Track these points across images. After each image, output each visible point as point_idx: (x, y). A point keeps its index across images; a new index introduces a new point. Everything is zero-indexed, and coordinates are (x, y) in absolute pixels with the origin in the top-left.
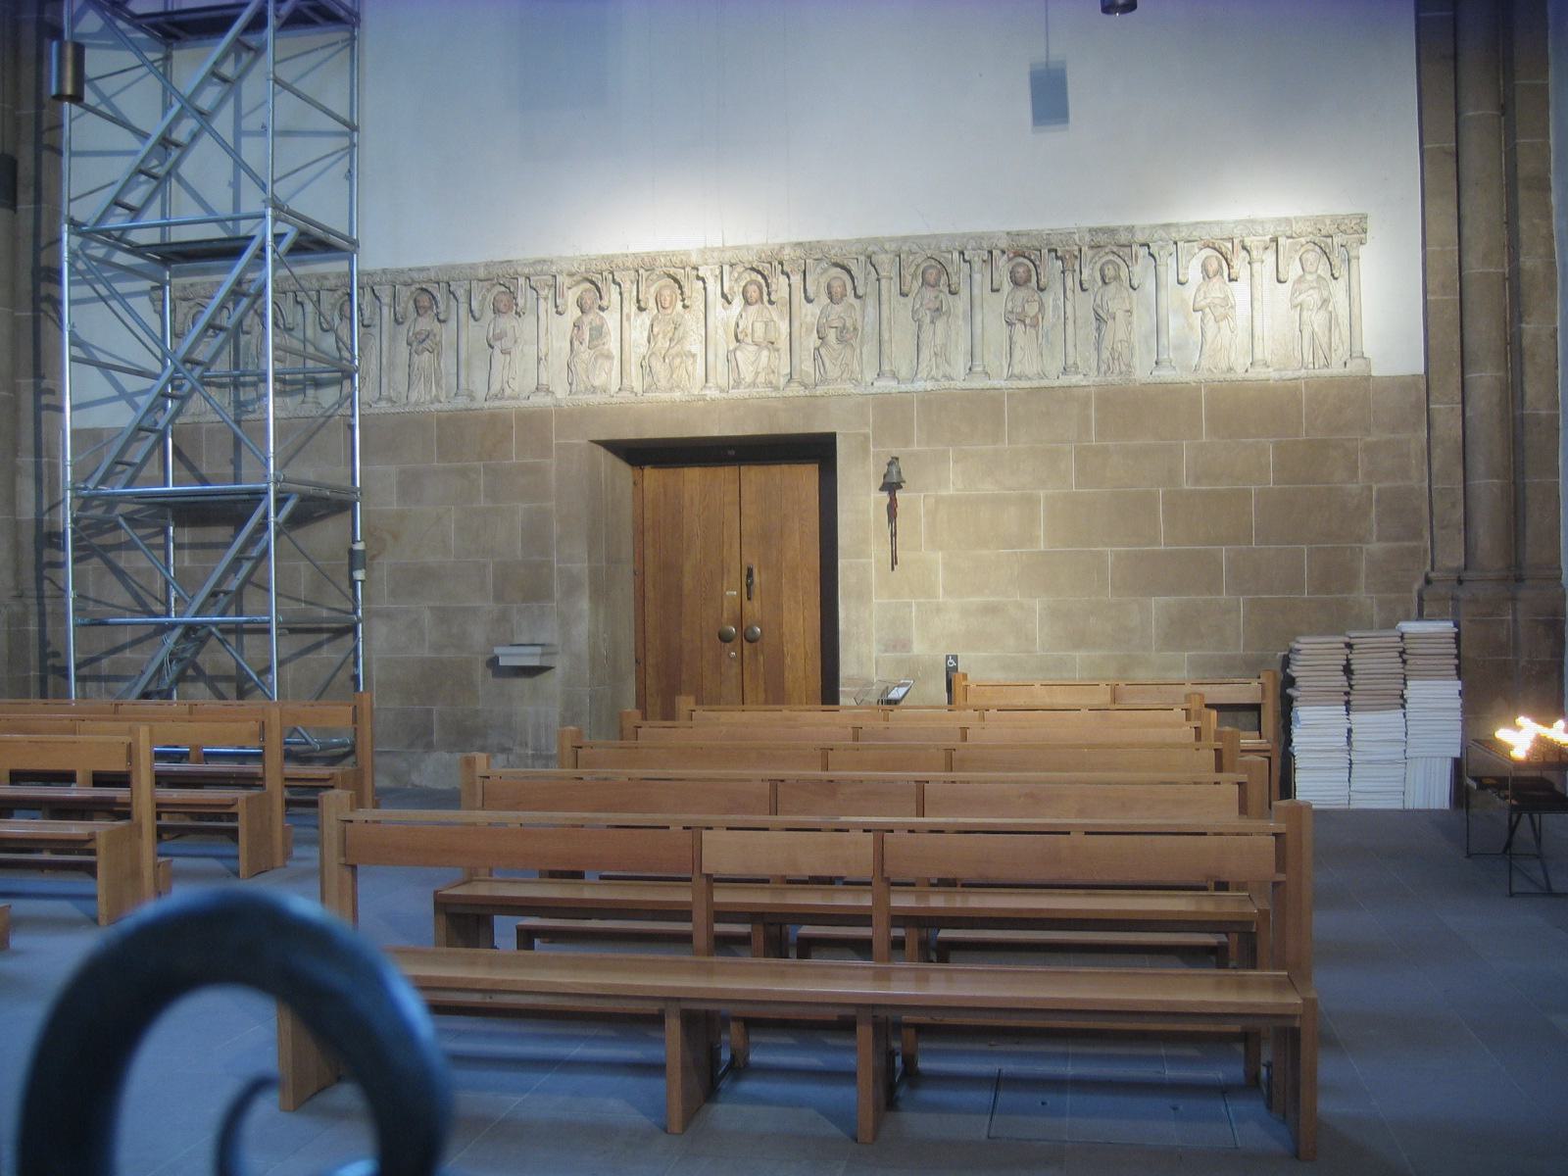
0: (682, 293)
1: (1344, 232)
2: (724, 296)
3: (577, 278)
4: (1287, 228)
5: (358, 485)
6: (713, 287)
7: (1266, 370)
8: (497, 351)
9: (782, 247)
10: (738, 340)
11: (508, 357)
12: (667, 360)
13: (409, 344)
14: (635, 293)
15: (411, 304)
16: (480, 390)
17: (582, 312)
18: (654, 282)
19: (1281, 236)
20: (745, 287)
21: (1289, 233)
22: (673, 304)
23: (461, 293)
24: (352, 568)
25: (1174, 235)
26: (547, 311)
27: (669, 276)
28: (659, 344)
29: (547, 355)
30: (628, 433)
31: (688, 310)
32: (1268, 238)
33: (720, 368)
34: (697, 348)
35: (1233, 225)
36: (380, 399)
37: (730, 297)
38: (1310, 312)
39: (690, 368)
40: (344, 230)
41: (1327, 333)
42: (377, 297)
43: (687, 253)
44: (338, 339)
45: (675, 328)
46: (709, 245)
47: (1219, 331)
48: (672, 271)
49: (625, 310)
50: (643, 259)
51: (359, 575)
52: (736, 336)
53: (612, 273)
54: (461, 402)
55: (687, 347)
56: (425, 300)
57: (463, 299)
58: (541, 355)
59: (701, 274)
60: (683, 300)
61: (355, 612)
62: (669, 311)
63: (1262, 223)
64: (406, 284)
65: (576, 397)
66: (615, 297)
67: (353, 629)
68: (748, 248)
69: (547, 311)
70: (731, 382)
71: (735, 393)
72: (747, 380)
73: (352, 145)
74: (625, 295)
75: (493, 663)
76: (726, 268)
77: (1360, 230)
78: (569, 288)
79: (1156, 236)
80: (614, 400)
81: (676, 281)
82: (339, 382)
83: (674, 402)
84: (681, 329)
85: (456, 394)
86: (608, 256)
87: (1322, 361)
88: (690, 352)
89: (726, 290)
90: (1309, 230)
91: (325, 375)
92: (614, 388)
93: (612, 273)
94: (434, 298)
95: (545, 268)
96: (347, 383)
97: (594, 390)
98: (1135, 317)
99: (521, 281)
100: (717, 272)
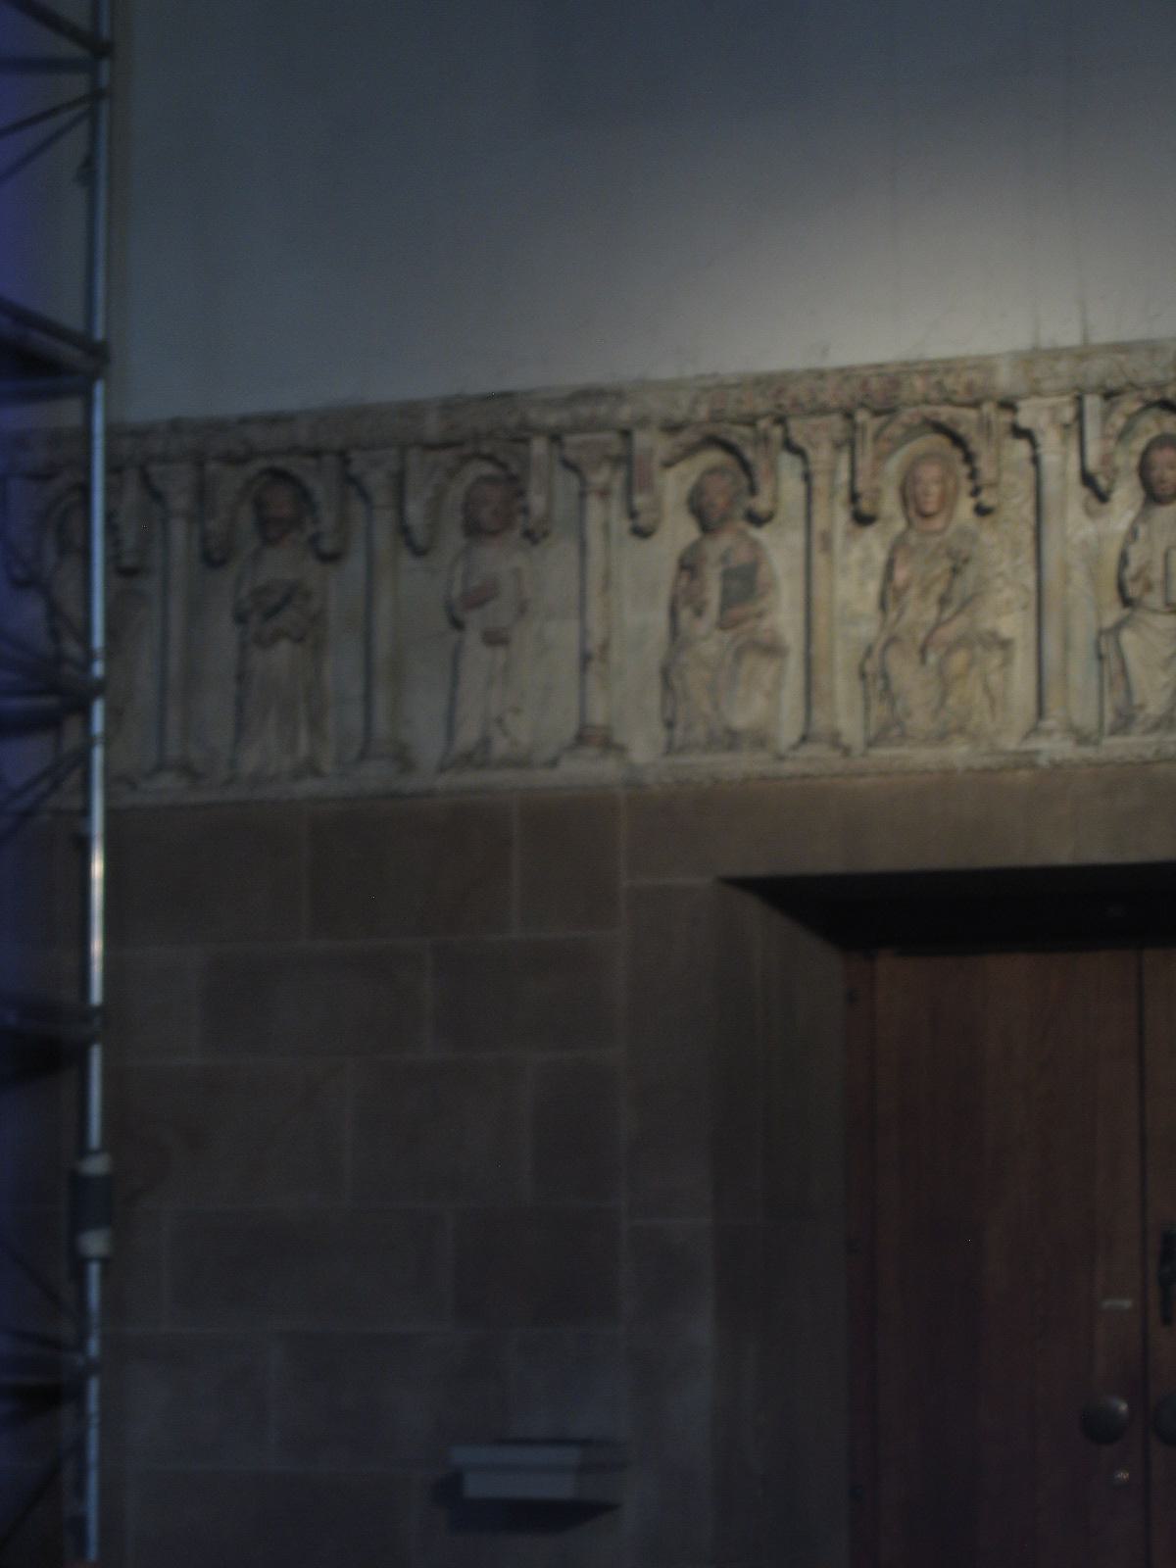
0: (973, 475)
2: (1087, 479)
3: (688, 437)
5: (96, 996)
6: (1058, 457)
8: (472, 638)
10: (1127, 602)
11: (500, 654)
12: (932, 659)
13: (241, 618)
14: (844, 476)
15: (246, 517)
16: (429, 749)
17: (707, 527)
18: (897, 444)
20: (1145, 455)
22: (947, 502)
23: (377, 480)
24: (77, 1227)
26: (606, 528)
27: (939, 428)
28: (910, 614)
29: (605, 647)
30: (824, 857)
31: (987, 521)
33: (1081, 672)
34: (1014, 624)
36: (160, 767)
37: (1102, 482)
39: (995, 679)
40: (70, 316)
42: (157, 496)
43: (984, 365)
44: (54, 611)
45: (955, 571)
46: (1045, 343)
48: (945, 413)
49: (820, 523)
50: (865, 384)
51: (95, 1243)
52: (1121, 588)
53: (781, 421)
54: (374, 776)
55: (987, 623)
56: (281, 502)
57: (382, 498)
58: (594, 643)
59: (1024, 419)
60: (975, 492)
61: (81, 1345)
62: (937, 523)
64: (233, 460)
66: (791, 487)
67: (79, 1395)
68: (1152, 348)
69: (606, 528)
70: (1109, 717)
71: (1117, 747)
73: (96, 95)
74: (820, 482)
75: (448, 1489)
76: (1093, 403)
78: (668, 465)
80: (788, 767)
81: (958, 441)
82: (50, 722)
83: (948, 772)
84: (970, 573)
85: (363, 756)
88: (994, 634)
89: (1093, 463)
91: (17, 704)
92: (788, 732)
93: (781, 421)
94: (304, 495)
95: (603, 410)
96: (72, 726)
97: (732, 740)
100: (1068, 414)
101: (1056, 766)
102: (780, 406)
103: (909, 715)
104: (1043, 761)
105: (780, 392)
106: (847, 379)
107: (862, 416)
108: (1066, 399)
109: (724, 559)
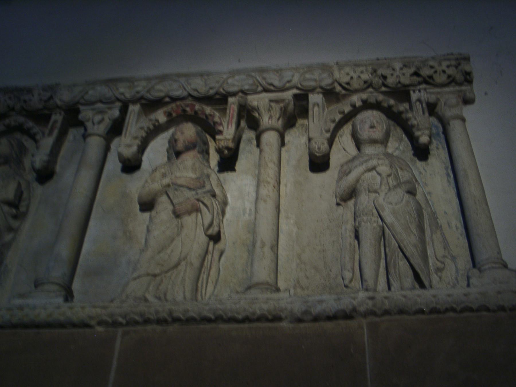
1: (428, 81)
4: (325, 75)
7: (275, 296)
19: (313, 90)
21: (326, 82)
25: (122, 90)
32: (288, 95)
35: (225, 77)
38: (373, 195)
41: (413, 228)
47: (178, 235)
63: (278, 71)
77: (459, 77)
79: (91, 92)
87: (409, 280)
90: (365, 77)
98: (27, 225)
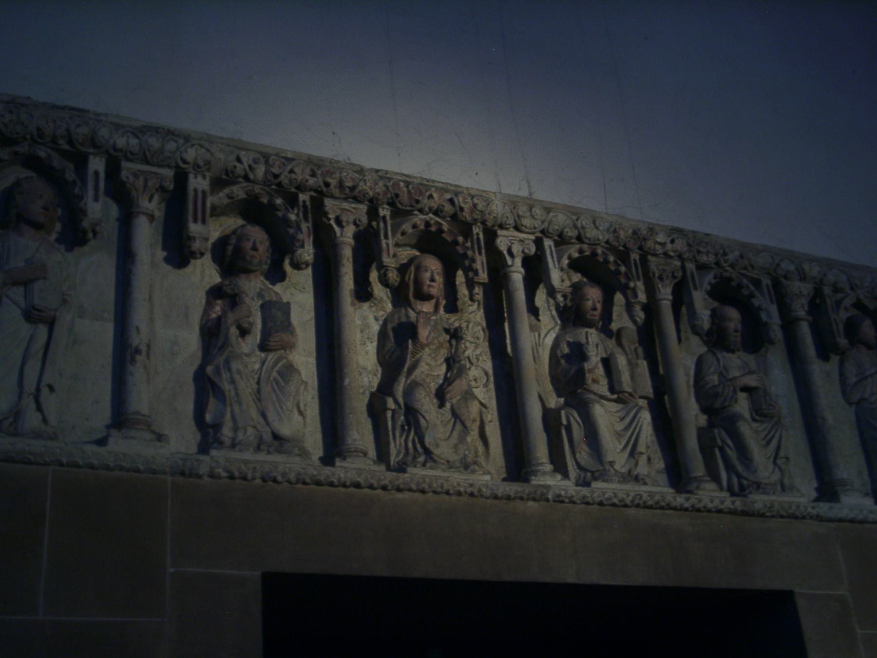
9: (651, 230)
28: (423, 368)
43: (483, 195)
65: (236, 455)
72: (617, 467)
86: (321, 159)
95: (171, 146)
99: (97, 164)
101: (559, 500)
102: (327, 185)
103: (437, 446)
104: (550, 496)
105: (330, 173)
106: (381, 178)
107: (385, 211)
108: (532, 237)
109: (260, 295)
